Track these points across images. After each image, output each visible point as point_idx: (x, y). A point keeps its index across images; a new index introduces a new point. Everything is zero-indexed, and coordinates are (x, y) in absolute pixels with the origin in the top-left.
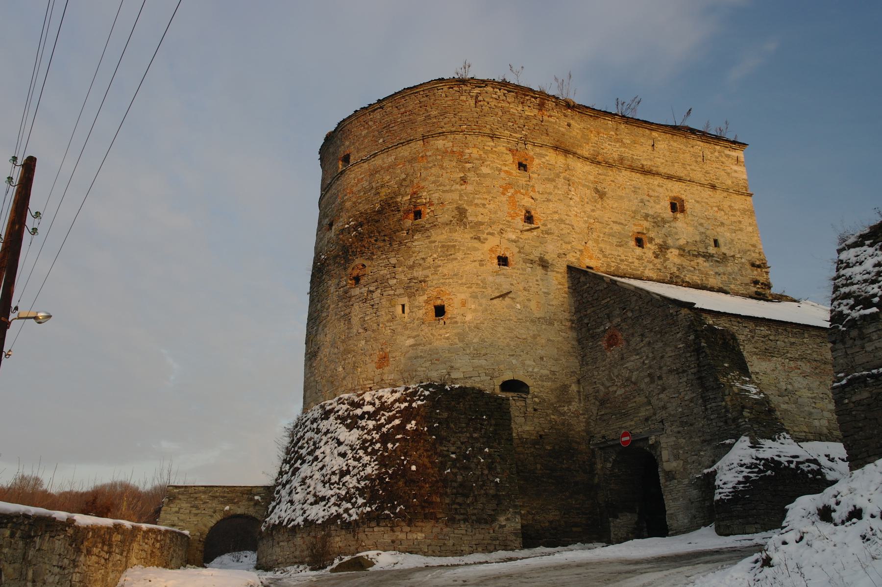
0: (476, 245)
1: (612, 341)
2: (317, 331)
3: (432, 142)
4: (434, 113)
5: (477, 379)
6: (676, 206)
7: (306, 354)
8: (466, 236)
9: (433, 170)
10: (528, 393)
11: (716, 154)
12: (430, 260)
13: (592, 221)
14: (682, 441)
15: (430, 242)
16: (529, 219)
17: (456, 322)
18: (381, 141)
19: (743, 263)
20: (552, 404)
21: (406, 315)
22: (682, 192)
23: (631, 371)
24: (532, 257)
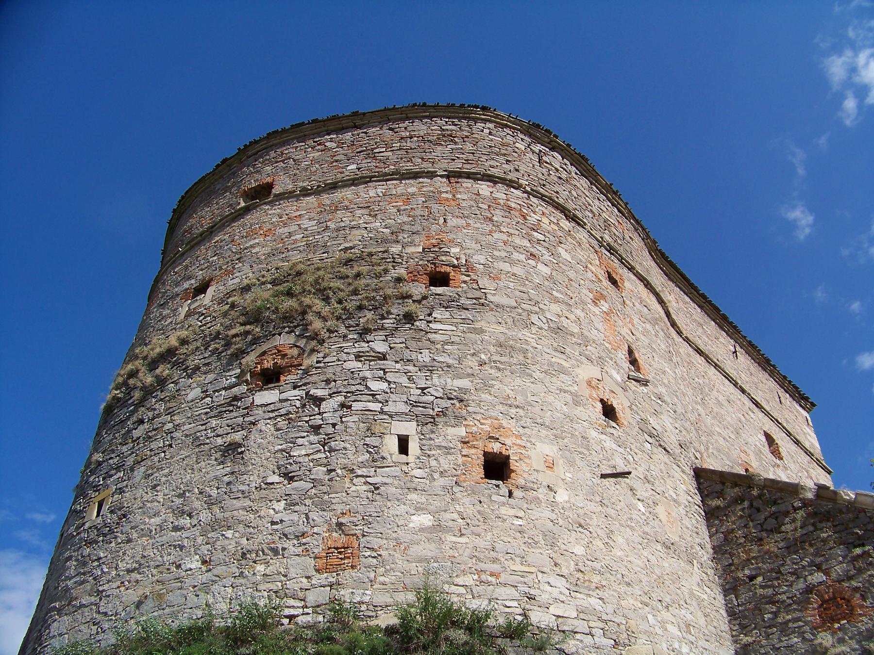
5: (588, 640)
8: (545, 341)
12: (472, 363)
21: (411, 458)
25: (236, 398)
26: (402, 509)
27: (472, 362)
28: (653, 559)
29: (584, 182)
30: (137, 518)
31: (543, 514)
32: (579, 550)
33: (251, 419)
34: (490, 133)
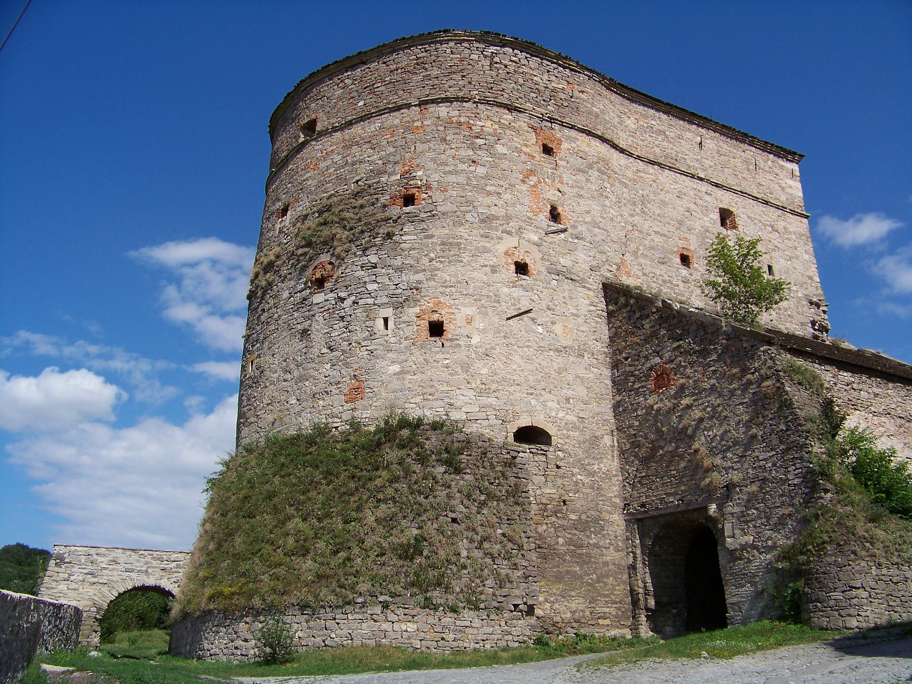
0: (488, 245)
3: (432, 108)
4: (435, 72)
5: (485, 423)
8: (475, 232)
11: (770, 163)
12: (425, 261)
13: (630, 228)
16: (555, 215)
18: (361, 103)
19: (800, 299)
20: (579, 461)
21: (389, 332)
22: (734, 204)
24: (559, 267)
26: (384, 363)
27: (425, 261)
28: (544, 364)
29: (534, 62)
30: (267, 373)
31: (461, 355)
32: (484, 371)
33: (311, 313)
34: (452, 53)
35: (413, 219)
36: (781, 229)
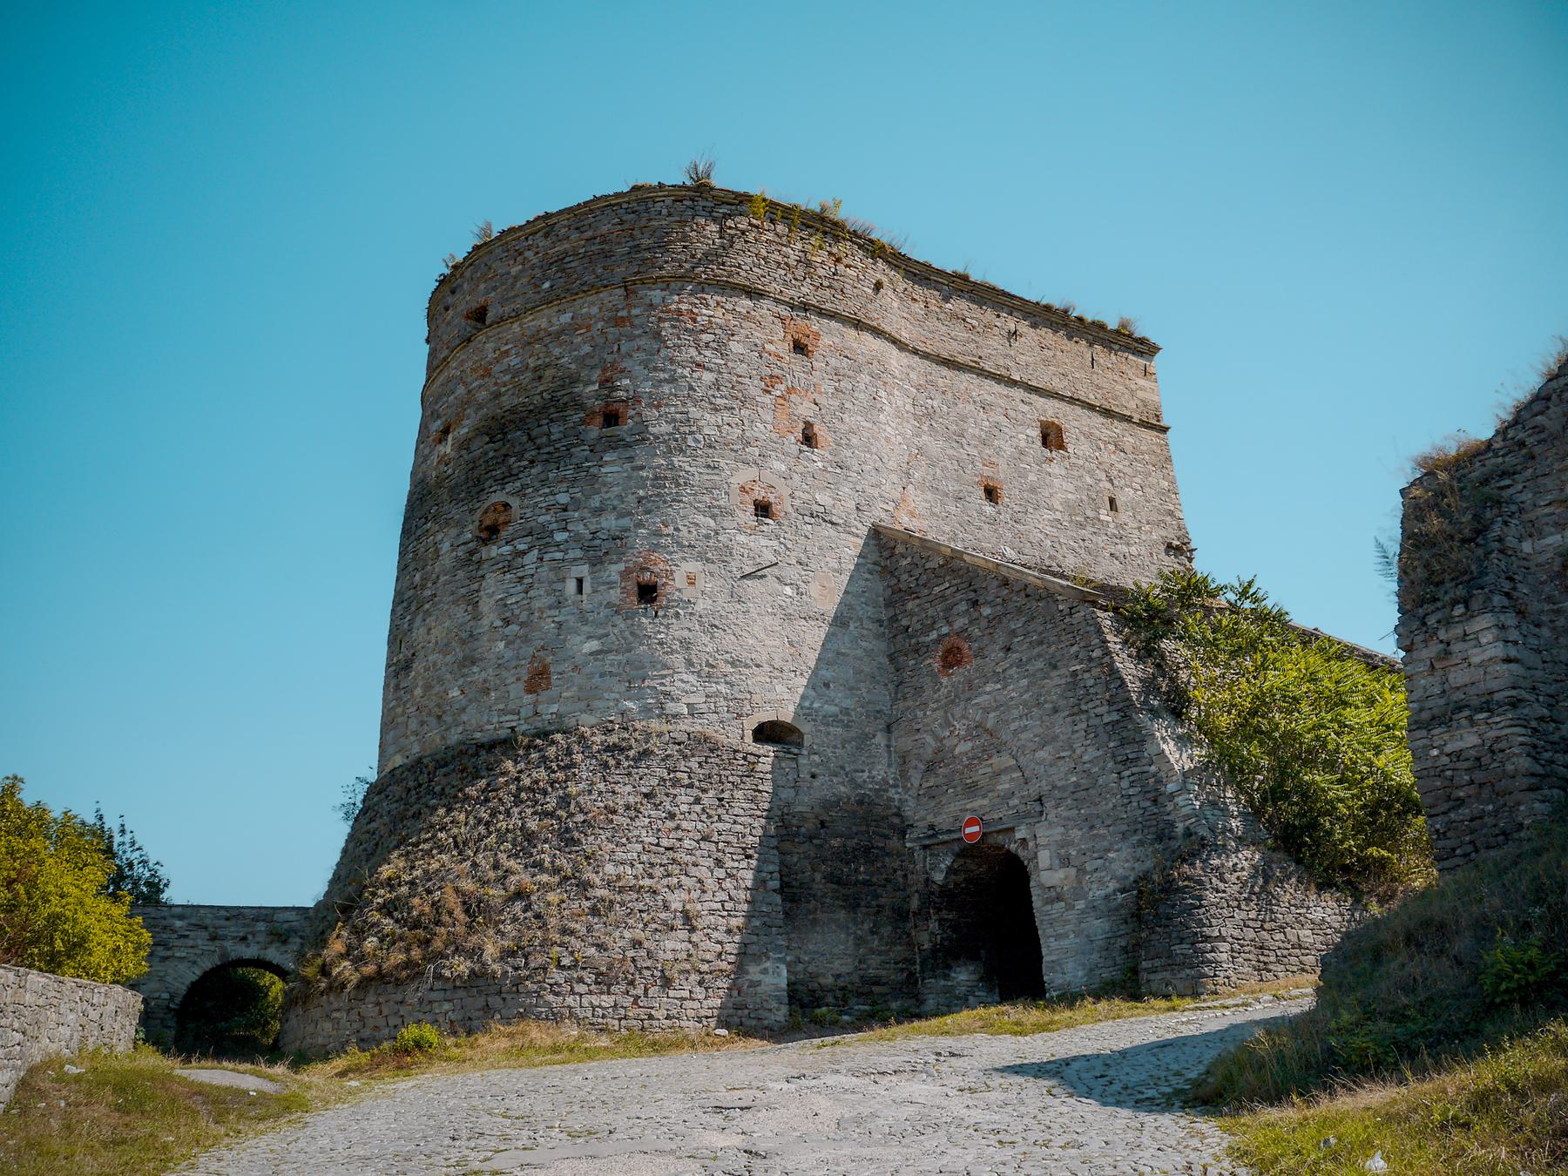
1: (952, 658)
2: (411, 622)
4: (646, 242)
6: (1051, 437)
7: (388, 666)
9: (641, 342)
10: (800, 745)
14: (1076, 834)
15: (633, 469)
16: (809, 439)
17: (677, 615)
18: (547, 285)
23: (987, 711)
24: (815, 507)
25: (471, 553)
26: (578, 639)
35: (615, 444)
36: (1128, 448)
